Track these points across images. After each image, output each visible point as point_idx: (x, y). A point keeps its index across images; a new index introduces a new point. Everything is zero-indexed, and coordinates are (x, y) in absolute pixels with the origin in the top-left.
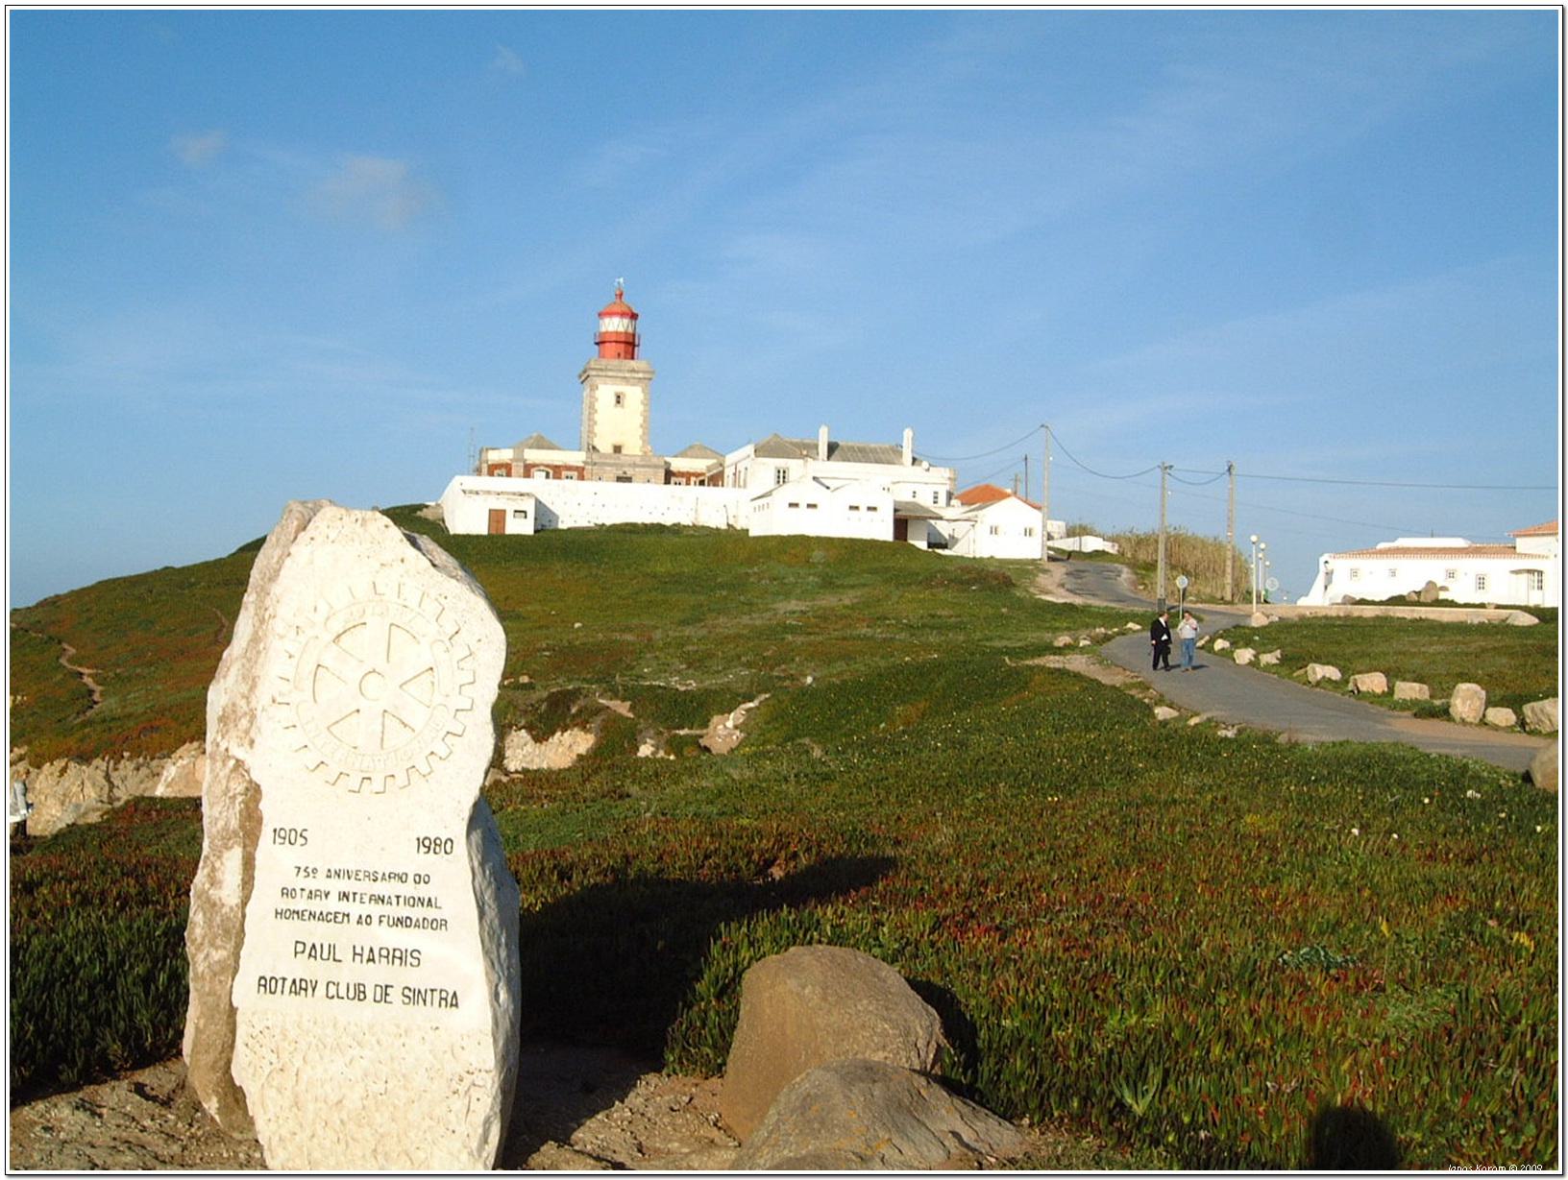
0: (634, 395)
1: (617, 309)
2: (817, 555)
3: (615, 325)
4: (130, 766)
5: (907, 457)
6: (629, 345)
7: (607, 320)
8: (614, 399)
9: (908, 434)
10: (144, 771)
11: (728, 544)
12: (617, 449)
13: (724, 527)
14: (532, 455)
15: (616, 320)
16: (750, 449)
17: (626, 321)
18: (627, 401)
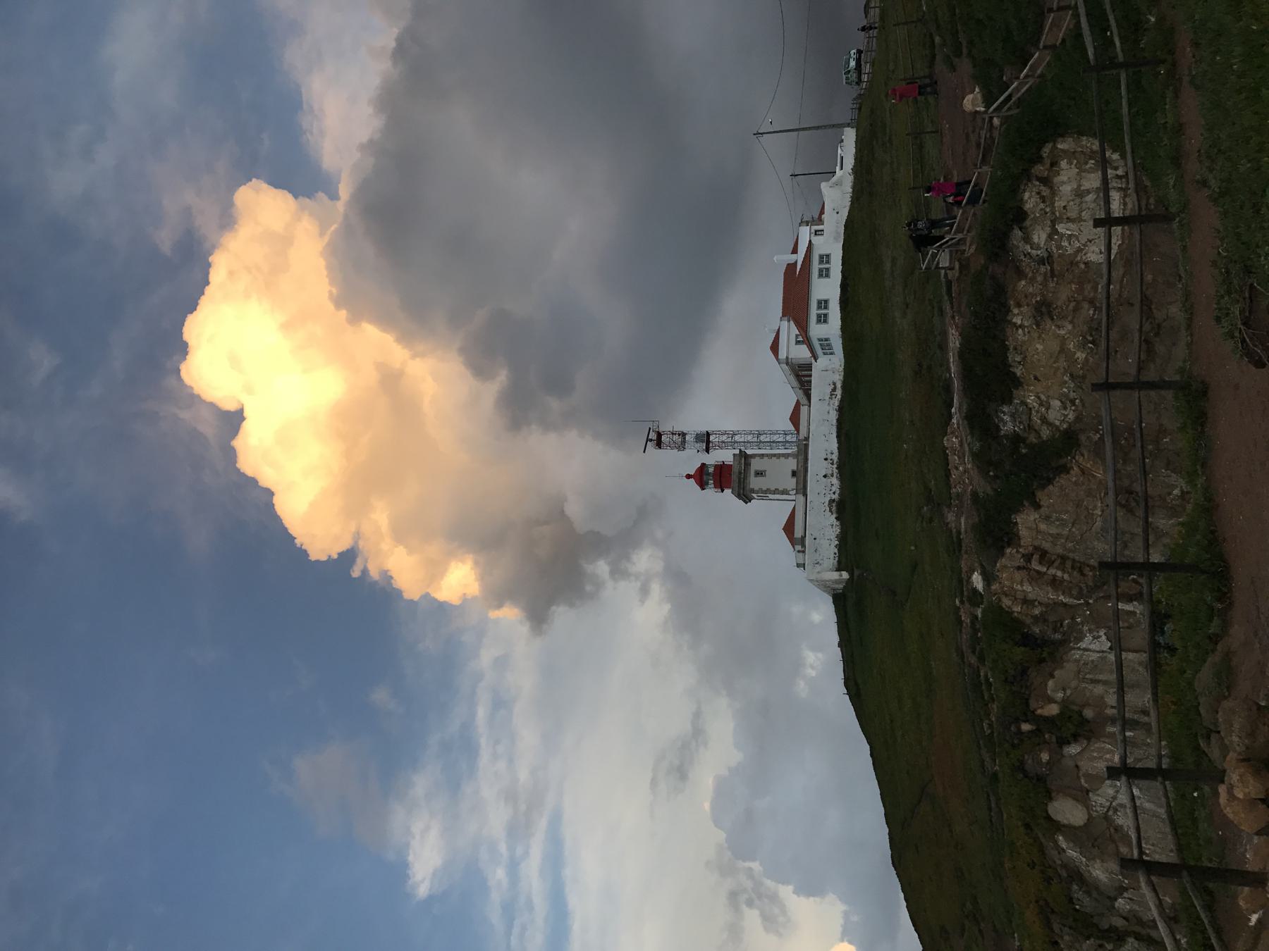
8: (760, 479)
18: (760, 468)
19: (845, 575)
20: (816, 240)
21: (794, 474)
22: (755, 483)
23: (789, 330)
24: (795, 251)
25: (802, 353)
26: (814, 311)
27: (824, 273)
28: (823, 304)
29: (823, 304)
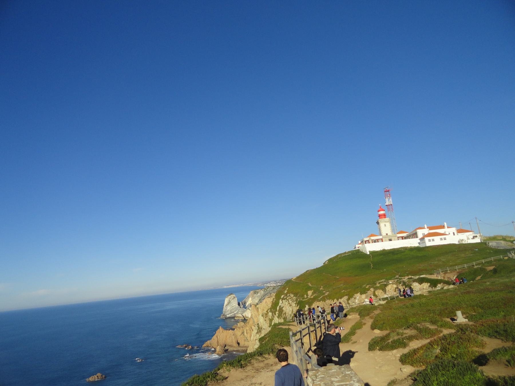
0: (388, 224)
12: (387, 234)
14: (373, 238)
19: (368, 253)
20: (452, 234)
23: (426, 231)
24: (448, 227)
25: (420, 235)
26: (431, 238)
27: (441, 239)
28: (433, 240)
29: (433, 240)
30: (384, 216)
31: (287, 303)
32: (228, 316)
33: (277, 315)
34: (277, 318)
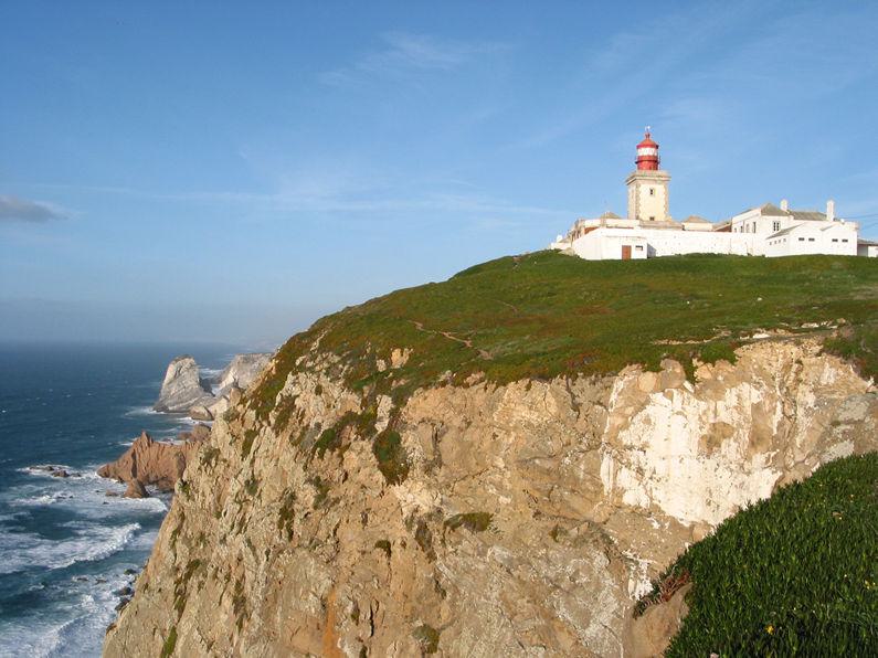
0: (660, 189)
1: (647, 142)
2: (836, 265)
3: (647, 152)
4: (586, 383)
5: (830, 216)
6: (654, 162)
7: (643, 149)
9: (830, 204)
10: (599, 385)
11: (762, 261)
13: (746, 255)
15: (648, 149)
16: (758, 211)
17: (653, 149)
21: (652, 219)
22: (645, 188)
30: (654, 162)
31: (311, 385)
32: (170, 408)
33: (273, 421)
34: (269, 429)
